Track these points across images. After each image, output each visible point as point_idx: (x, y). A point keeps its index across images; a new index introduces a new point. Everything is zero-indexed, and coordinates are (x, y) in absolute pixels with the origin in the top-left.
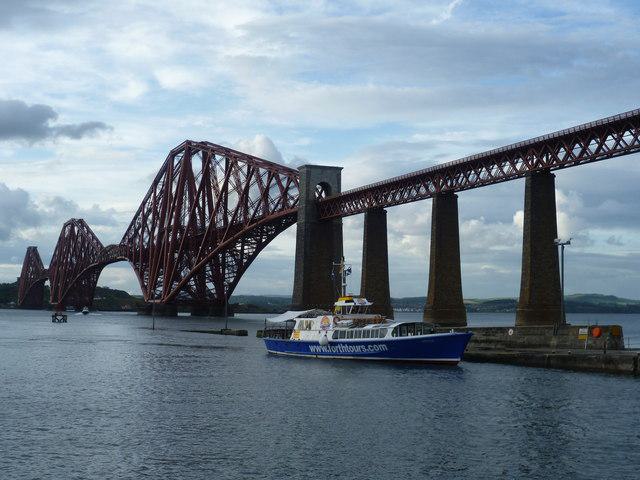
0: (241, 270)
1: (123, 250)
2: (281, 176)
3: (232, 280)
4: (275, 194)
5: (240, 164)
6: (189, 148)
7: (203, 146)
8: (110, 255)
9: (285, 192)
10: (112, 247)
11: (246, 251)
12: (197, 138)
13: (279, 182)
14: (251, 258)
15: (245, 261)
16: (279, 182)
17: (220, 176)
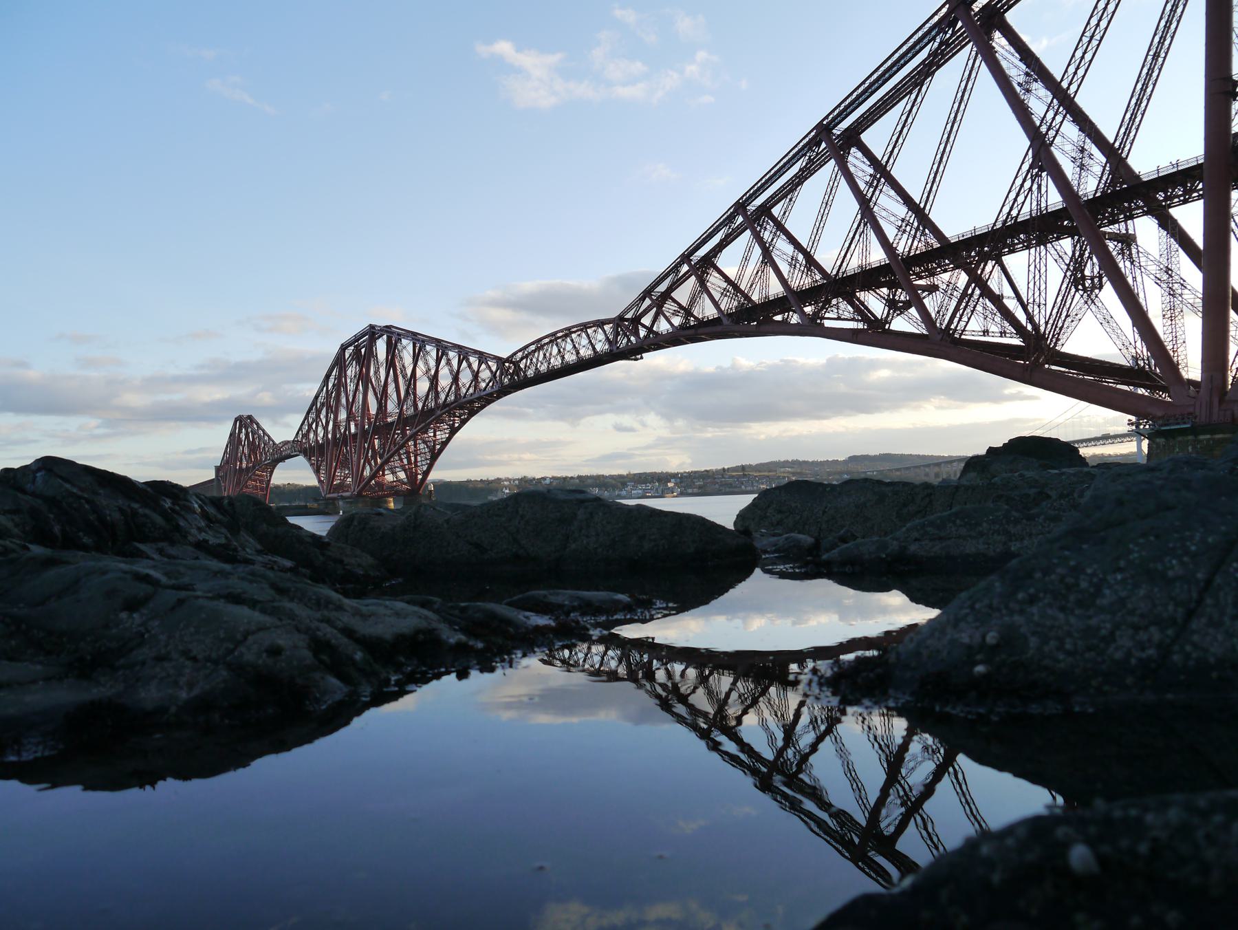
0: (435, 456)
1: (300, 447)
2: (472, 359)
3: (425, 468)
4: (465, 378)
5: (428, 348)
6: (372, 333)
7: (388, 330)
8: (281, 454)
9: (476, 376)
10: (286, 443)
11: (438, 437)
12: (381, 322)
13: (470, 366)
14: (444, 444)
15: (438, 447)
16: (470, 366)
17: (408, 359)
